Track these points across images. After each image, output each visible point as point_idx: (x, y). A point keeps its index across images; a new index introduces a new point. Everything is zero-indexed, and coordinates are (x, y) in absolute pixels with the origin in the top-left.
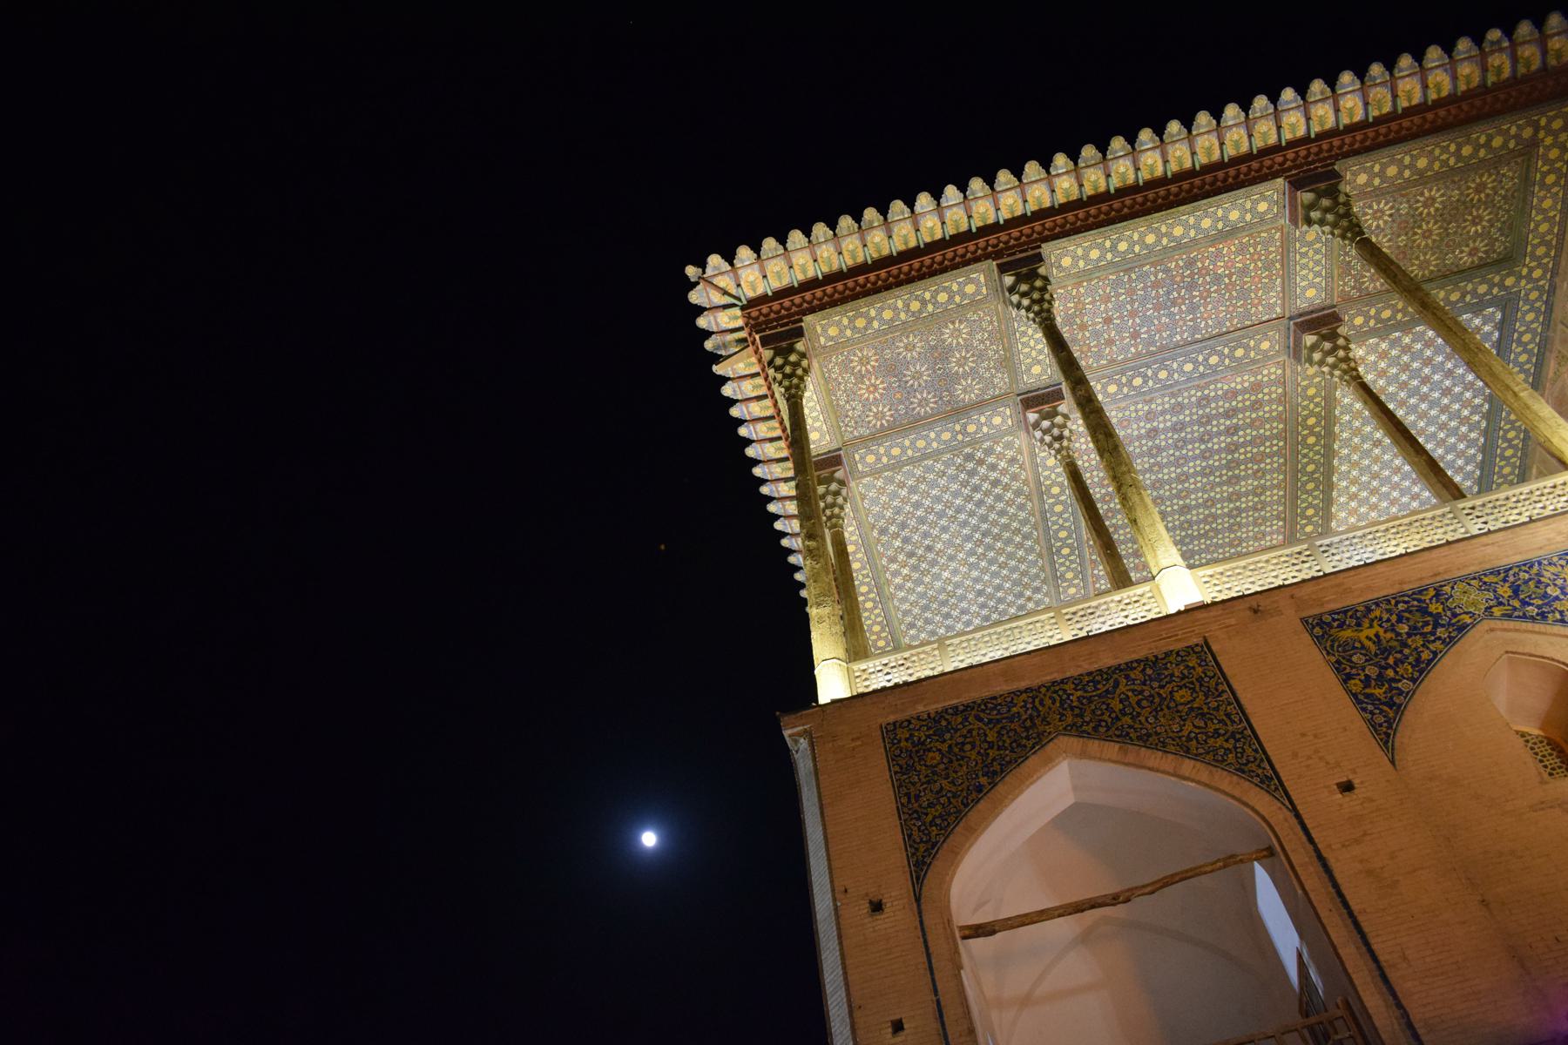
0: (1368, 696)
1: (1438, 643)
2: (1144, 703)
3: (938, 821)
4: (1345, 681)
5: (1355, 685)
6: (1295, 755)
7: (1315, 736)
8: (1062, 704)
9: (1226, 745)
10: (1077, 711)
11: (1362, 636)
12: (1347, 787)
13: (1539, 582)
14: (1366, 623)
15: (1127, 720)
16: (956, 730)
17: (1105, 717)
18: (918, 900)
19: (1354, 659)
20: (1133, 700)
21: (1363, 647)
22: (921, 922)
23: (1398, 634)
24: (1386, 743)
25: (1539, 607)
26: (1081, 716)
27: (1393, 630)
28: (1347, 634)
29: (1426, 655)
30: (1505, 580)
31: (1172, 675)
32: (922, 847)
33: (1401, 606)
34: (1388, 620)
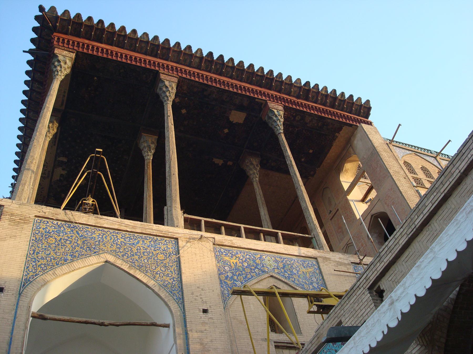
0: (225, 282)
1: (255, 273)
2: (146, 254)
3: (43, 266)
4: (220, 274)
5: (223, 277)
6: (192, 294)
7: (202, 290)
8: (113, 241)
9: (169, 281)
10: (118, 246)
11: (232, 261)
12: (205, 311)
13: (292, 266)
14: (234, 257)
15: (137, 257)
16: (66, 234)
17: (129, 253)
18: (20, 294)
19: (226, 268)
20: (142, 251)
21: (230, 265)
22: (18, 304)
23: (243, 266)
24: (225, 301)
25: (289, 274)
26: (120, 249)
27: (242, 263)
28: (227, 258)
29: (249, 276)
30: (282, 262)
31: (160, 248)
32: (31, 274)
33: (248, 256)
34: (242, 260)
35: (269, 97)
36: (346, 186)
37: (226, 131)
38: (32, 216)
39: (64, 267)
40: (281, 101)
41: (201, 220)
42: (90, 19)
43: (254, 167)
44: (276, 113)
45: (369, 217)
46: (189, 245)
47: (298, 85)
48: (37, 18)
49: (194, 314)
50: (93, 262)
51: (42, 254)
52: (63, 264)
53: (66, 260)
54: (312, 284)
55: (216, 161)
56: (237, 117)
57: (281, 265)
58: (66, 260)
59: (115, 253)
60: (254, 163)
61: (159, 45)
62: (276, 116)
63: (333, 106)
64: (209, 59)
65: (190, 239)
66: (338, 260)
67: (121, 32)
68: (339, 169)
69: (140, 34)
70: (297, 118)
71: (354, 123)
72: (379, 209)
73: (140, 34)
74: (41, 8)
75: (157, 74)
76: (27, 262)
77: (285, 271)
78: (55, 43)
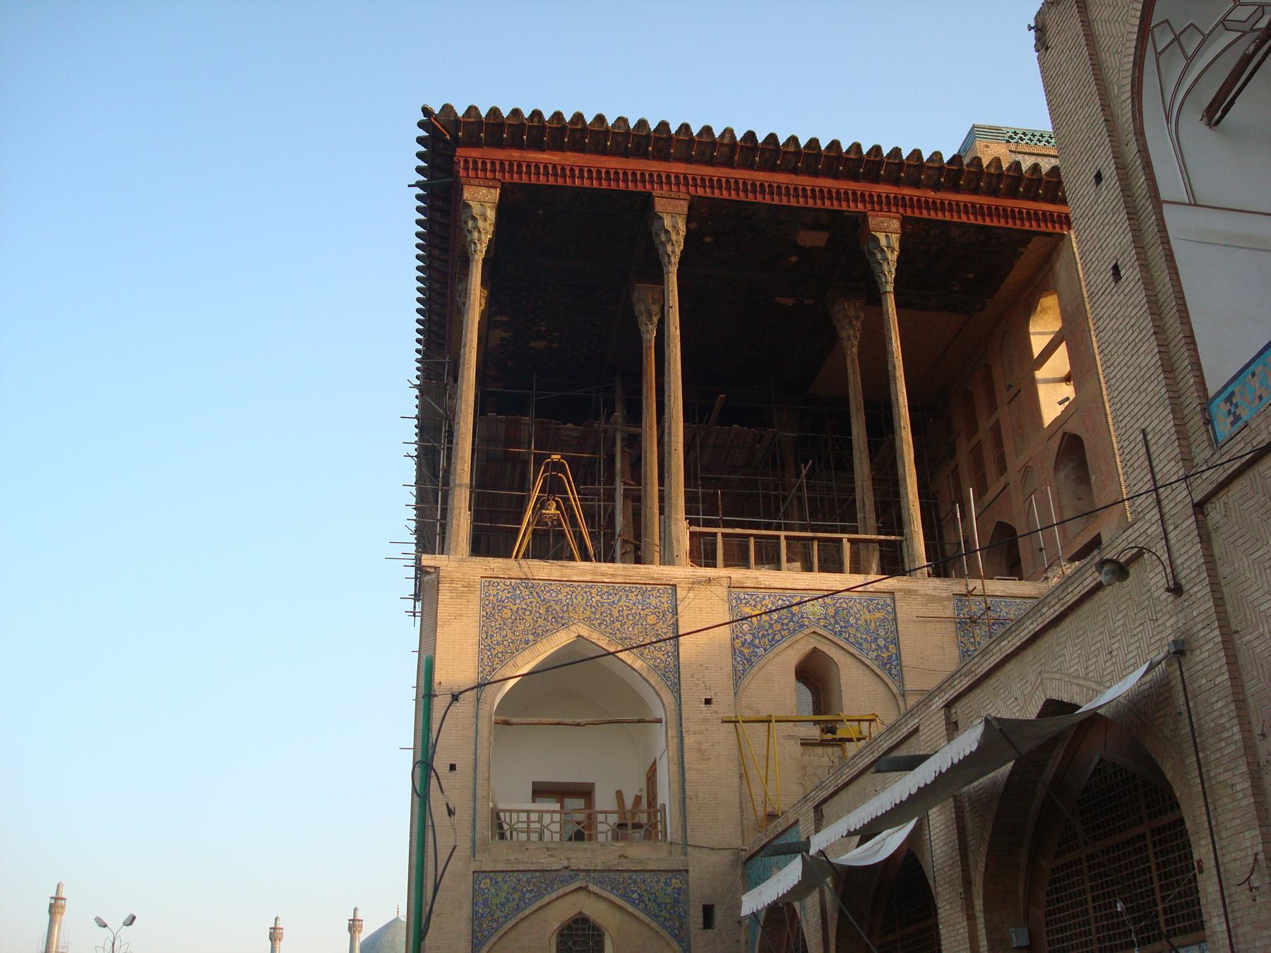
0: (741, 652)
5: (738, 643)
12: (708, 702)
15: (618, 624)
20: (626, 613)
29: (777, 637)
32: (488, 669)
35: (872, 202)
36: (1038, 344)
37: (794, 259)
38: (478, 579)
39: (526, 653)
40: (896, 205)
41: (715, 534)
42: (516, 112)
43: (851, 323)
44: (883, 242)
45: (1060, 434)
46: (691, 594)
47: (936, 165)
48: (421, 125)
49: (692, 706)
50: (562, 639)
51: (497, 638)
52: (524, 649)
53: (527, 642)
54: (876, 639)
55: (781, 300)
56: (813, 239)
57: (831, 611)
58: (527, 642)
59: (589, 621)
60: (851, 313)
61: (648, 136)
62: (882, 251)
63: (1013, 194)
64: (749, 145)
65: (693, 583)
66: (929, 592)
67: (577, 124)
68: (1028, 309)
69: (610, 121)
70: (932, 233)
71: (1058, 230)
72: (1073, 427)
73: (610, 121)
74: (426, 111)
75: (648, 199)
76: (481, 651)
77: (836, 622)
78: (462, 173)
